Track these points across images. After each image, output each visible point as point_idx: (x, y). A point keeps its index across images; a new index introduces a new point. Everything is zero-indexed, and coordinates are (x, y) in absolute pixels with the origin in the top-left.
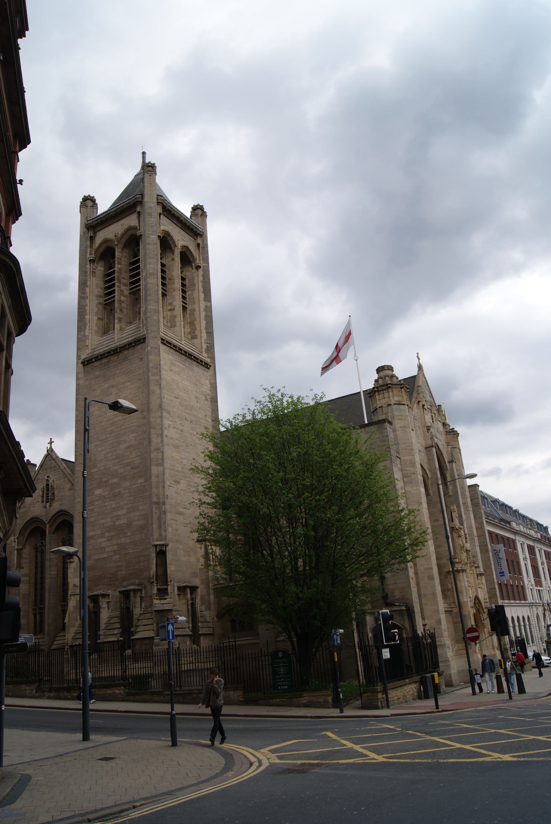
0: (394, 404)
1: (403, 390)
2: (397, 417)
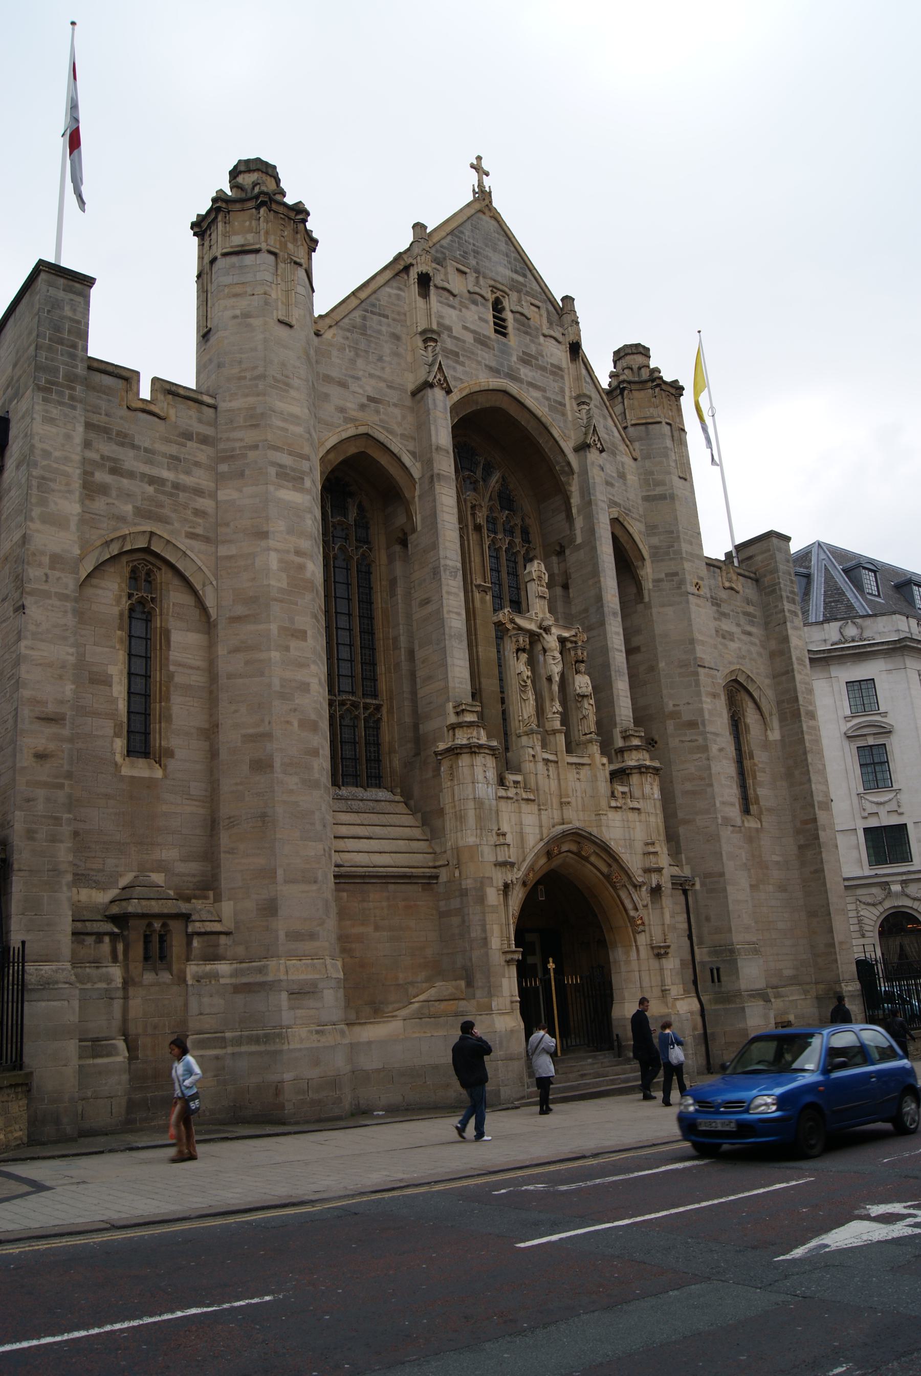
0: (225, 255)
1: (262, 210)
2: (226, 291)
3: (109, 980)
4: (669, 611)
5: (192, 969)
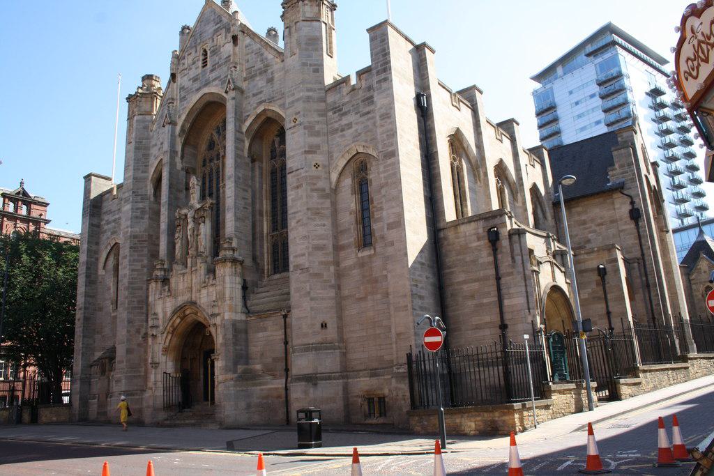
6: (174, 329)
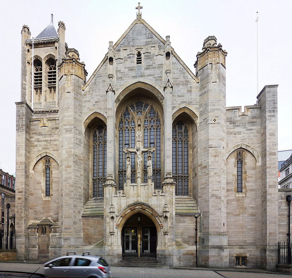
3: (36, 236)
4: (203, 132)
5: (51, 234)
6: (125, 215)
